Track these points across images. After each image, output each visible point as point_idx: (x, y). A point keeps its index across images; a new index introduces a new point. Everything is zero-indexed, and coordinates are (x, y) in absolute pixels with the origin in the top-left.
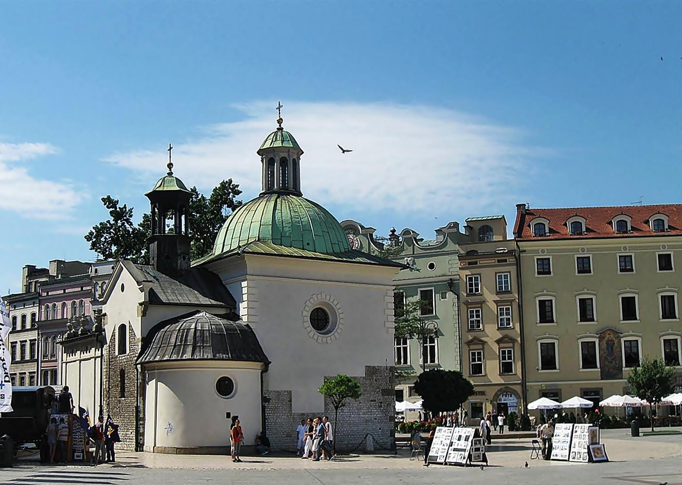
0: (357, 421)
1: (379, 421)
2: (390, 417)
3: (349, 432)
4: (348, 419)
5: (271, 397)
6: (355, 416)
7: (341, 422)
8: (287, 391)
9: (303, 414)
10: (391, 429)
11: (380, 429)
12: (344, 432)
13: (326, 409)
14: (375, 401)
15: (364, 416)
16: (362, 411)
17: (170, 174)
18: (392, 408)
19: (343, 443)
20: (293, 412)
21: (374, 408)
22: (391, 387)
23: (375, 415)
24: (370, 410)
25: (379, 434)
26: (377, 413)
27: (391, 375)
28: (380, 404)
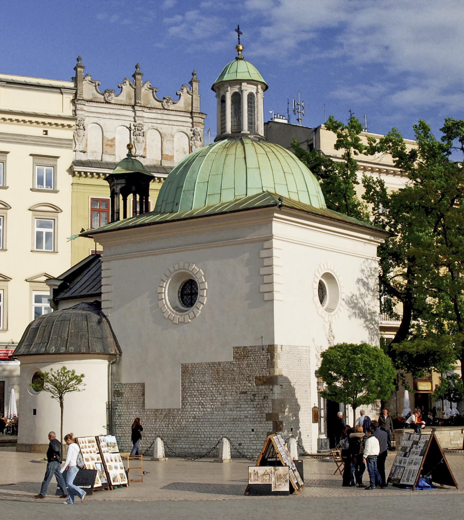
0: (222, 420)
1: (252, 420)
2: (267, 414)
3: (212, 433)
4: (209, 417)
5: (124, 391)
6: (220, 412)
7: (202, 420)
8: (140, 383)
9: (157, 410)
10: (268, 431)
11: (253, 430)
12: (205, 433)
13: (183, 404)
14: (246, 393)
15: (231, 412)
16: (228, 406)
17: (130, 155)
18: (270, 402)
19: (203, 447)
20: (146, 408)
21: (246, 403)
22: (269, 374)
23: (246, 412)
24: (239, 406)
25: (250, 438)
26: (249, 409)
27: (269, 356)
28: (252, 397)
